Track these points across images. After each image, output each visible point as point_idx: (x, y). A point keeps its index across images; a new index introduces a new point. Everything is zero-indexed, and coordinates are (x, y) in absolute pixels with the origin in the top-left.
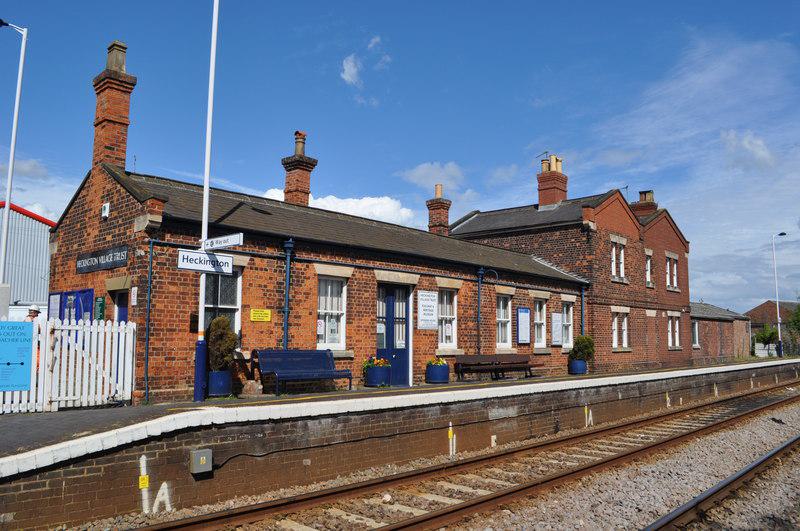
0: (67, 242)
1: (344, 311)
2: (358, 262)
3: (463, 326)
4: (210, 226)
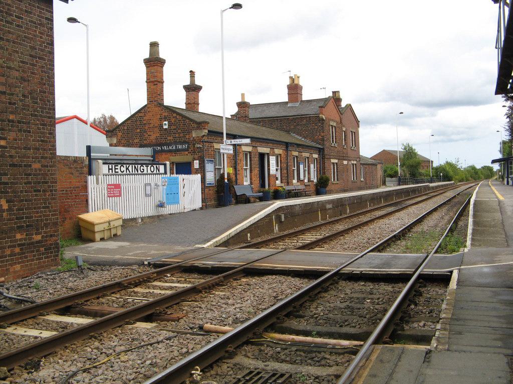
1: (249, 167)
2: (254, 144)
4: (227, 134)
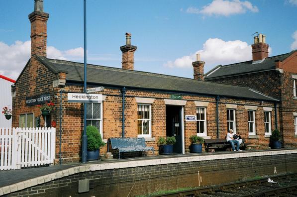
0: (21, 91)
2: (157, 96)
3: (209, 125)
